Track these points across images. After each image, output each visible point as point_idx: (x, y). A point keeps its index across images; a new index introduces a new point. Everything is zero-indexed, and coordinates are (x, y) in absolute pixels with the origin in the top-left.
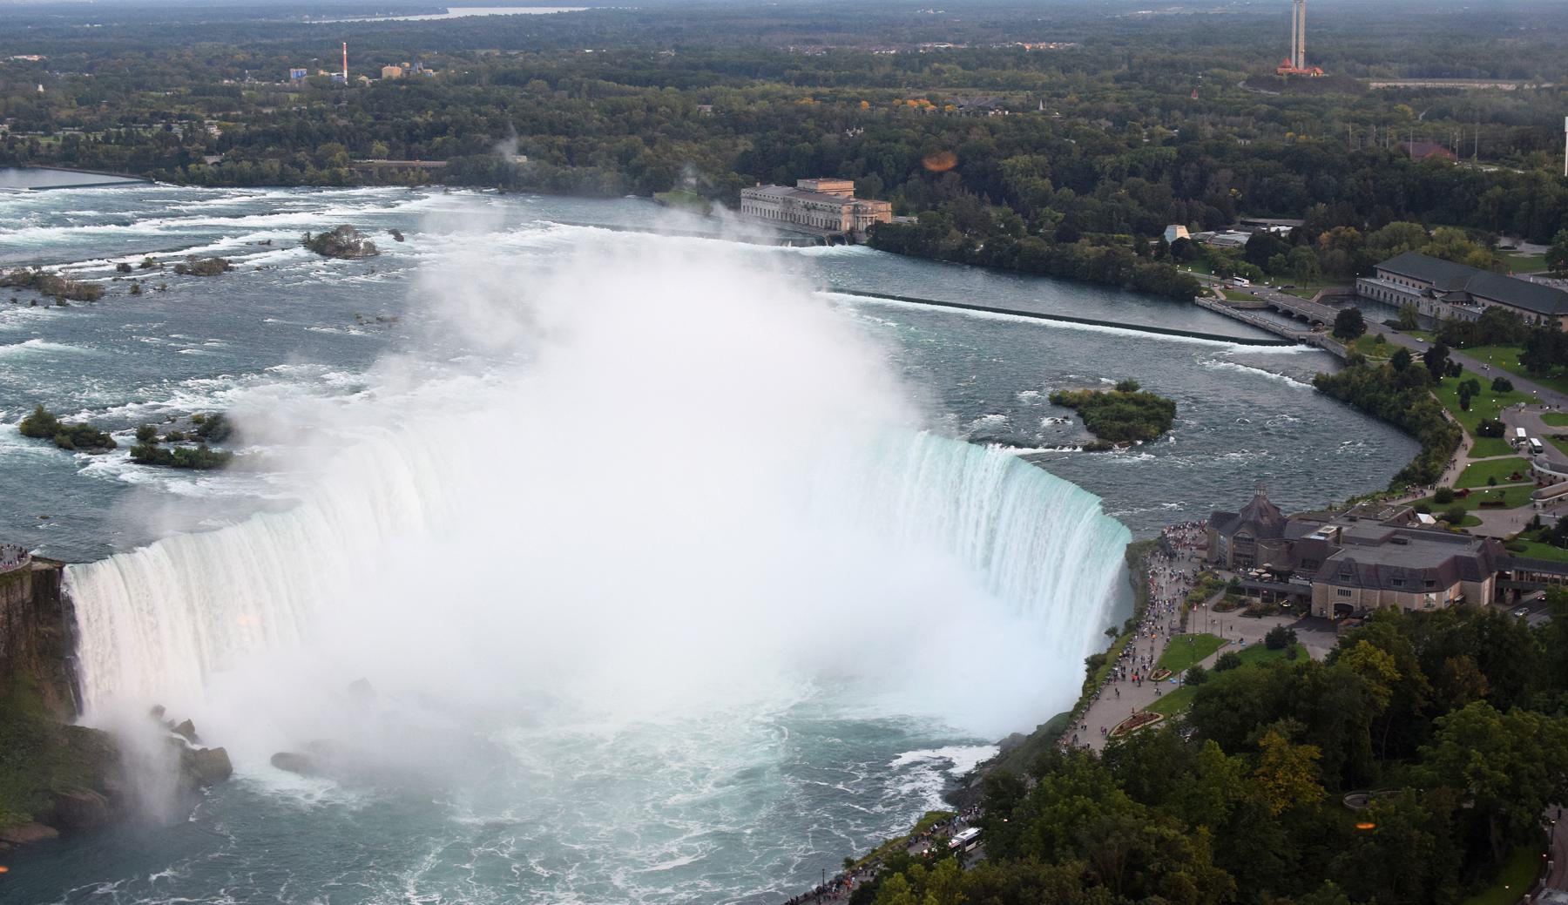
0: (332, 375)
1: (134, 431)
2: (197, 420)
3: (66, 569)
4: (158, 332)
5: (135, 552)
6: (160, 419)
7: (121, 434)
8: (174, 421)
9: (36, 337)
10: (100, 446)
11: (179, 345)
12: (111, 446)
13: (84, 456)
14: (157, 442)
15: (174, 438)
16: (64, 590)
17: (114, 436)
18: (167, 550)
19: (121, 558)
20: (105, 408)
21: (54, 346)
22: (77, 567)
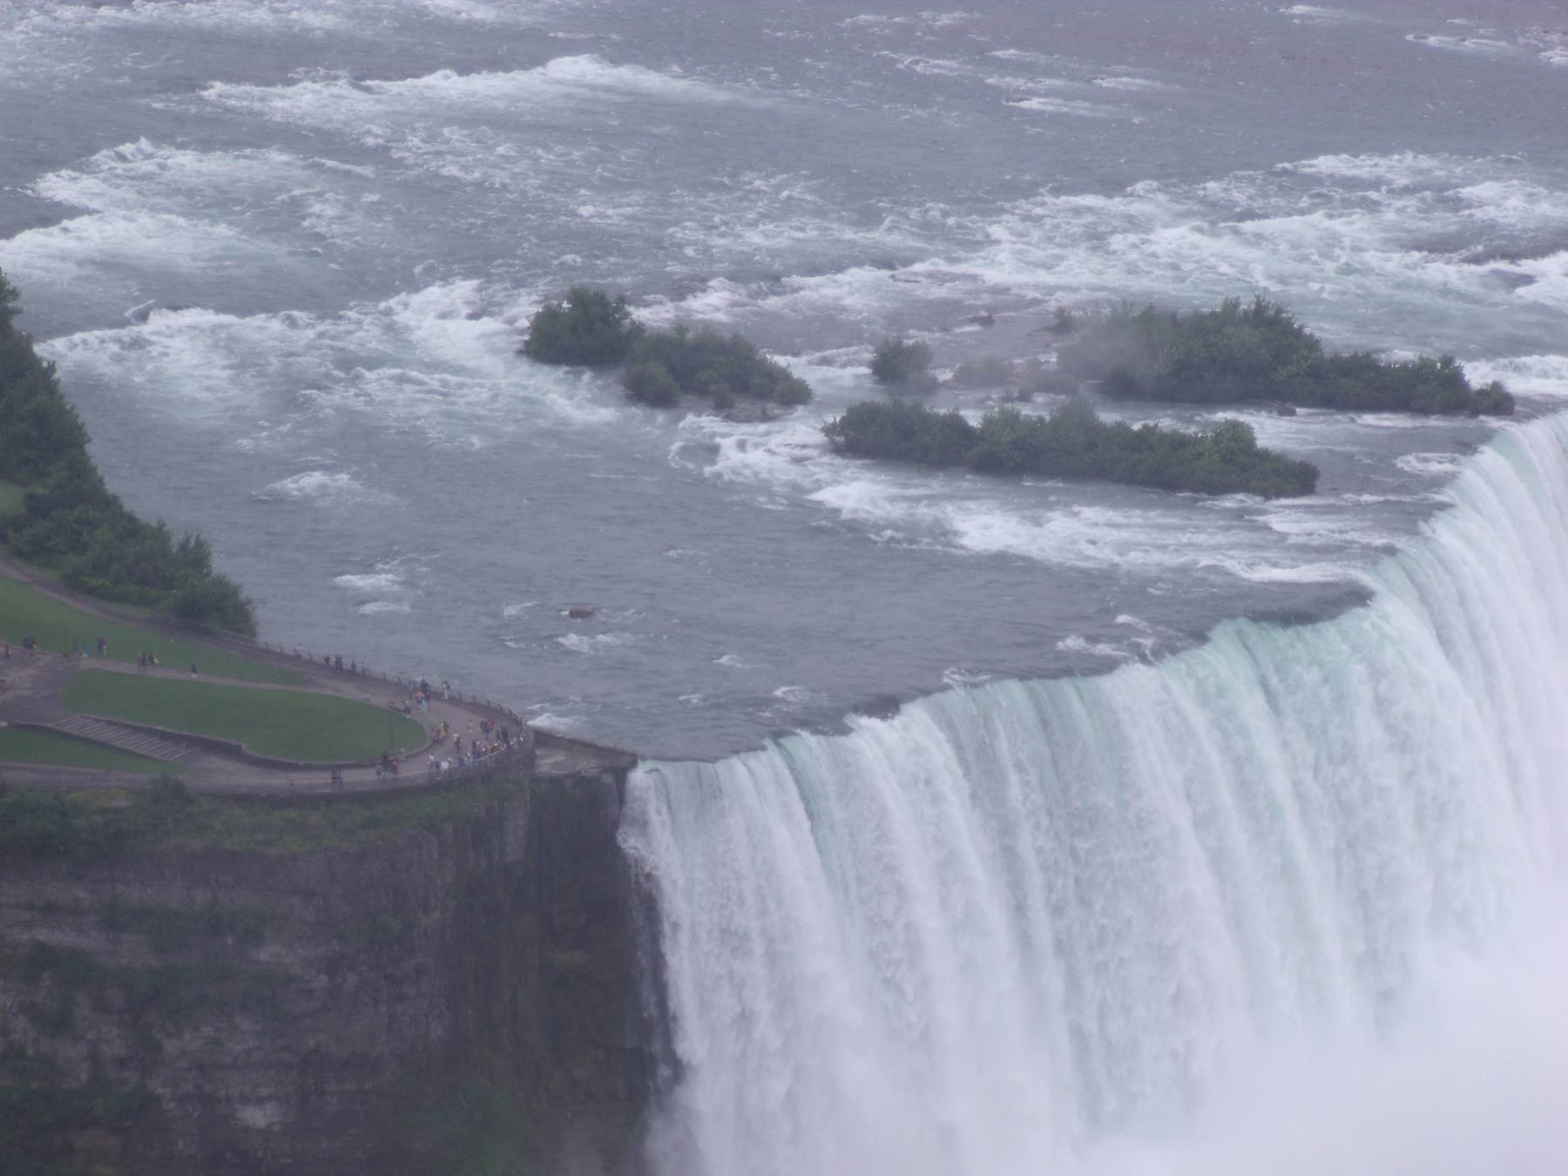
0: (1484, 190)
1: (869, 356)
2: (1063, 324)
3: (639, 777)
4: (948, 43)
5: (845, 731)
6: (943, 314)
7: (826, 362)
8: (987, 322)
9: (572, 48)
10: (763, 394)
11: (1020, 83)
12: (794, 395)
13: (708, 423)
14: (932, 387)
15: (973, 377)
16: (629, 842)
17: (799, 367)
18: (948, 724)
19: (807, 744)
20: (775, 278)
21: (628, 75)
22: (668, 769)
